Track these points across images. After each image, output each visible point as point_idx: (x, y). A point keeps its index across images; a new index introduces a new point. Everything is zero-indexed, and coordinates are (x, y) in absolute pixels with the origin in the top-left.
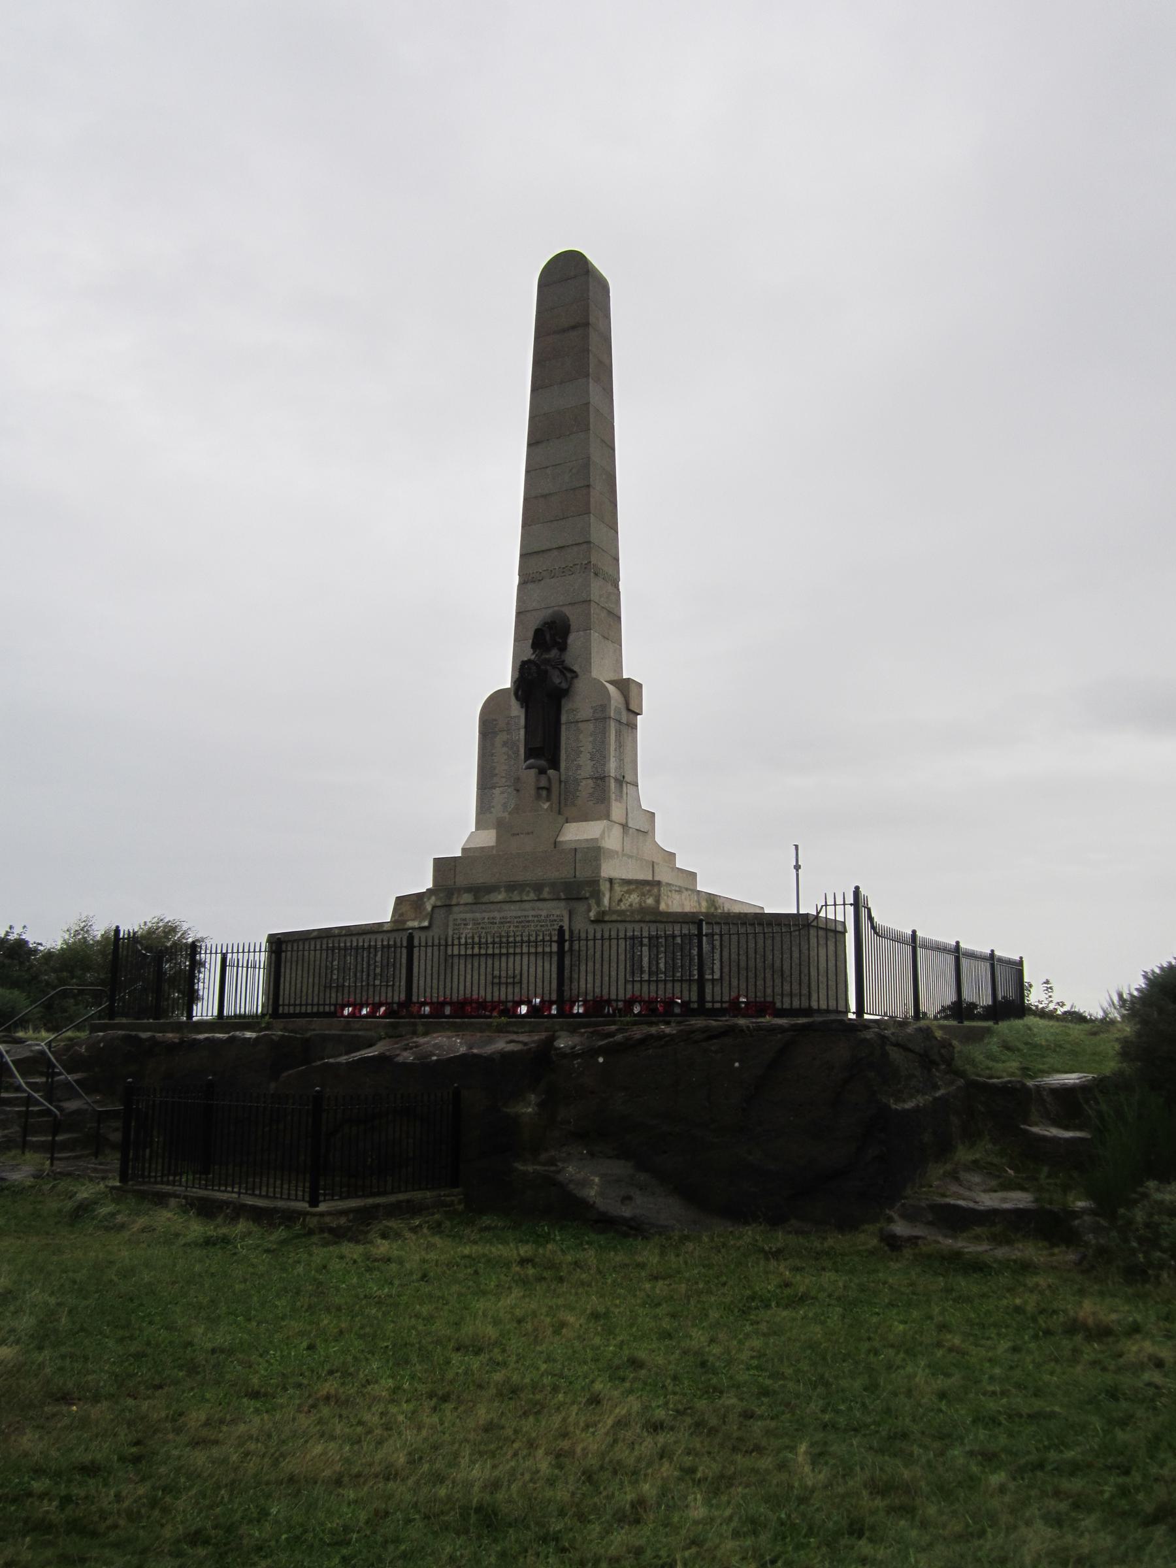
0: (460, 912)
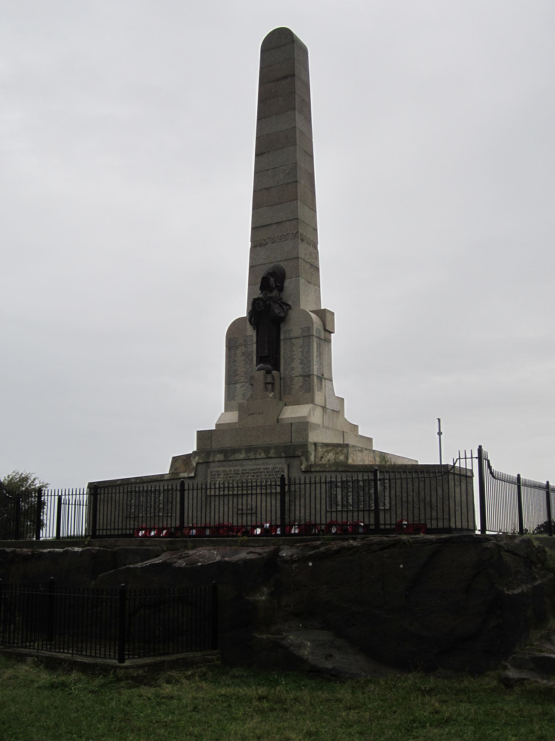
0: (216, 467)
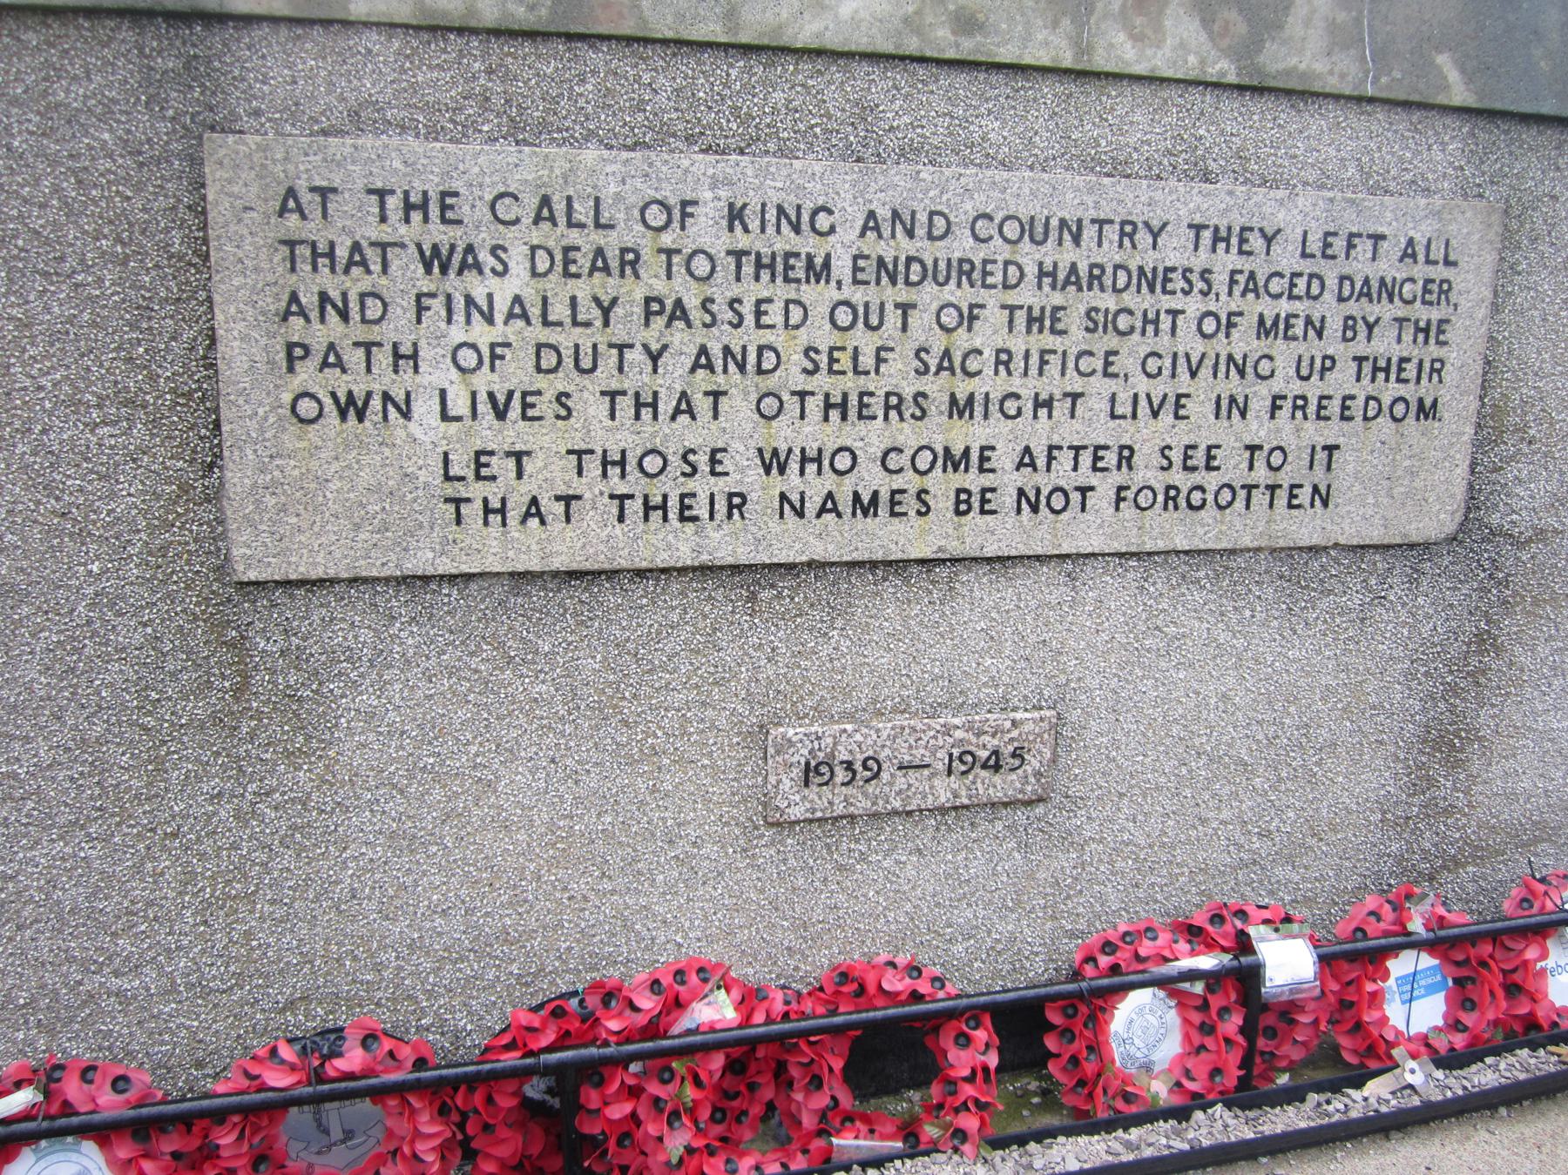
0: (359, 119)
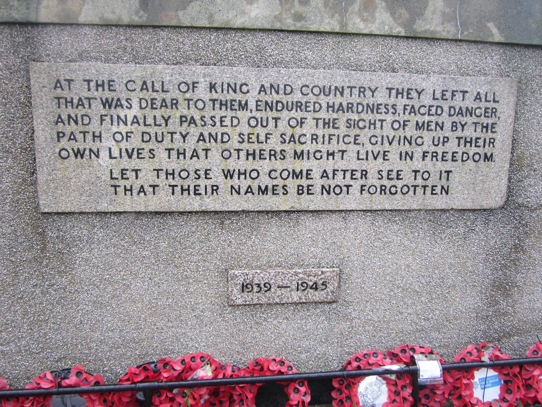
0: (82, 56)
